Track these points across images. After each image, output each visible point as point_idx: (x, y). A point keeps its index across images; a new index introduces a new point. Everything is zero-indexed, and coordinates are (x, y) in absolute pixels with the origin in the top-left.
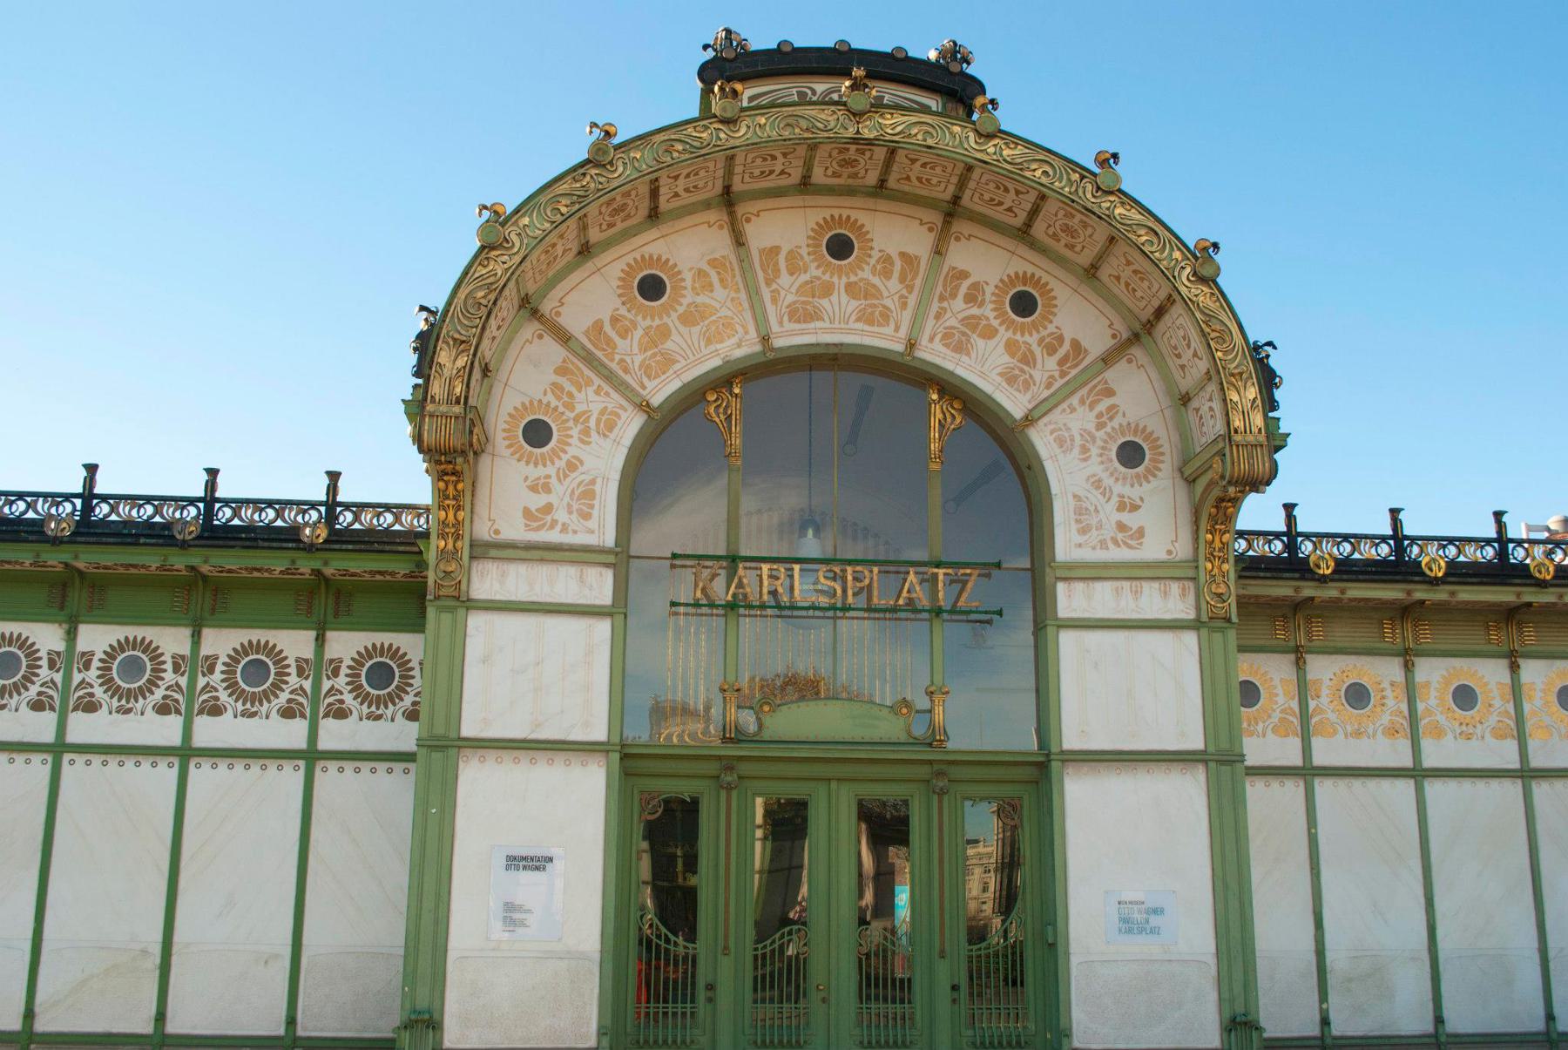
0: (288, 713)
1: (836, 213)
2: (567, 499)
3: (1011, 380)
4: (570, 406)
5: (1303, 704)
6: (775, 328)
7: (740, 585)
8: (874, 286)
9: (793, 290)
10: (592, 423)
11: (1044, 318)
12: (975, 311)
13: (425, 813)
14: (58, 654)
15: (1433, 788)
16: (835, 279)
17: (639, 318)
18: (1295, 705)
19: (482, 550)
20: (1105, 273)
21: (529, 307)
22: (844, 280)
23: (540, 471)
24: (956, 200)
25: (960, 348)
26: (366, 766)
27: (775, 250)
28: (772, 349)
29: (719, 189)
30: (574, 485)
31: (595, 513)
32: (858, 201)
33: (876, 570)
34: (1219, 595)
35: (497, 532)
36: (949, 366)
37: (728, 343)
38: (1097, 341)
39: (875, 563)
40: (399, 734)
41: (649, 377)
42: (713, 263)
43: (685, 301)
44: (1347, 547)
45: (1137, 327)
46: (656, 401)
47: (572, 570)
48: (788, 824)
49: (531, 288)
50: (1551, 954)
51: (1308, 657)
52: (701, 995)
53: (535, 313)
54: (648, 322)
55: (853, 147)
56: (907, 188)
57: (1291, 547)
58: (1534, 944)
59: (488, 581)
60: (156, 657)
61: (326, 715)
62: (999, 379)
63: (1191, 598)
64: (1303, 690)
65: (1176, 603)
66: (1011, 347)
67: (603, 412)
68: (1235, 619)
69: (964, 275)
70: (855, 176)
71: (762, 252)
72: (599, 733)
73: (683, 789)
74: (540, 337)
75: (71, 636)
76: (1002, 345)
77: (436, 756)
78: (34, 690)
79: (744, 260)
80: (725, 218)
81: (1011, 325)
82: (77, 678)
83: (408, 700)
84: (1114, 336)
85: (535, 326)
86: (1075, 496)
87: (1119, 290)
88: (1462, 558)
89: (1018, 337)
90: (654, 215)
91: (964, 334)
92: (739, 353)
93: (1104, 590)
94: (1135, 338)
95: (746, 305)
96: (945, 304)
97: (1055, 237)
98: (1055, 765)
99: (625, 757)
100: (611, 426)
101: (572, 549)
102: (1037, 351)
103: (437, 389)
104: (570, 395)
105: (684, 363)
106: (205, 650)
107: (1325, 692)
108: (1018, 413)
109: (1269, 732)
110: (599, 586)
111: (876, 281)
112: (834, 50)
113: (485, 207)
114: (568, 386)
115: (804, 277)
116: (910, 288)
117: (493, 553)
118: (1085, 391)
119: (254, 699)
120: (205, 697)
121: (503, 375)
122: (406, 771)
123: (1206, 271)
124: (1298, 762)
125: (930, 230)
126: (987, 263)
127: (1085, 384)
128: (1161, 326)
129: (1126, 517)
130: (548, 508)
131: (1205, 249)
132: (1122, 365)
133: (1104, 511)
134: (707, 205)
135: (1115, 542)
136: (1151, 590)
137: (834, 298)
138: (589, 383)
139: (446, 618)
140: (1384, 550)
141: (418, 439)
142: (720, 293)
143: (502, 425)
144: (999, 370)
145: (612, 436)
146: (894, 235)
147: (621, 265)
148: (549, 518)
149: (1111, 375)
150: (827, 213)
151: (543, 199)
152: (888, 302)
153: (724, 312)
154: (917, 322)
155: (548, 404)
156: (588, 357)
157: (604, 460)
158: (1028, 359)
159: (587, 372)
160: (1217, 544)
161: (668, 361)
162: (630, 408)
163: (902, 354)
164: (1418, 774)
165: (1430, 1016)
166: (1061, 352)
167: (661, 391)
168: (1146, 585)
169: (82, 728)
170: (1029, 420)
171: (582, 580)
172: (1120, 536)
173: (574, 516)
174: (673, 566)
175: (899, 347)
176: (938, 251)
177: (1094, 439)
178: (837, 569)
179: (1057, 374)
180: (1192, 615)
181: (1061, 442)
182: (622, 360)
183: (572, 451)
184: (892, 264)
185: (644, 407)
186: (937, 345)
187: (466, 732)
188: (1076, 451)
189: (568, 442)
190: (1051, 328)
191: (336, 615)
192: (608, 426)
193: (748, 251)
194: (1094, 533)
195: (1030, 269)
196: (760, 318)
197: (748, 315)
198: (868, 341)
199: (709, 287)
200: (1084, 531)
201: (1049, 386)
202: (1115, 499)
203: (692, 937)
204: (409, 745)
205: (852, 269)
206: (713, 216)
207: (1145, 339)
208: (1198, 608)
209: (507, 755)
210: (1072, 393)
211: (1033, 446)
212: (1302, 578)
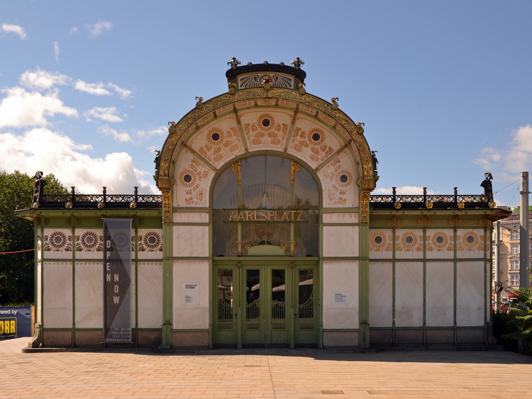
3: (312, 158)
4: (196, 171)
5: (394, 243)
6: (249, 146)
7: (241, 216)
11: (322, 141)
12: (303, 140)
13: (166, 275)
15: (428, 264)
16: (265, 132)
18: (391, 243)
19: (176, 210)
21: (184, 145)
23: (189, 189)
25: (299, 150)
31: (203, 199)
36: (296, 155)
38: (336, 147)
40: (158, 255)
42: (232, 129)
43: (225, 140)
47: (198, 214)
48: (253, 277)
50: (457, 307)
52: (234, 317)
53: (185, 145)
54: (215, 147)
59: (177, 218)
63: (357, 217)
64: (394, 238)
65: (354, 219)
66: (313, 149)
67: (204, 172)
69: (300, 129)
71: (245, 125)
72: (207, 255)
75: (73, 232)
77: (168, 261)
78: (66, 246)
79: (241, 128)
83: (160, 246)
89: (314, 146)
90: (215, 116)
92: (239, 154)
93: (335, 215)
95: (241, 140)
98: (321, 261)
99: (214, 261)
100: (206, 175)
101: (198, 208)
102: (319, 150)
104: (196, 168)
107: (400, 239)
108: (314, 168)
110: (206, 218)
111: (276, 132)
112: (263, 64)
114: (195, 166)
115: (257, 132)
116: (285, 134)
117: (178, 210)
118: (332, 161)
121: (178, 164)
122: (160, 264)
126: (306, 125)
129: (342, 196)
130: (191, 198)
132: (342, 154)
133: (337, 195)
134: (230, 113)
135: (339, 203)
136: (347, 216)
137: (265, 137)
138: (200, 164)
139: (168, 227)
142: (234, 137)
143: (178, 177)
147: (207, 131)
150: (262, 113)
152: (279, 138)
153: (235, 143)
156: (200, 157)
157: (206, 184)
158: (317, 152)
159: (200, 161)
160: (365, 203)
161: (221, 157)
164: (425, 260)
165: (422, 322)
167: (219, 165)
168: (346, 214)
169: (79, 255)
170: (317, 169)
172: (340, 201)
173: (198, 200)
175: (283, 151)
176: (293, 122)
177: (334, 174)
180: (357, 222)
181: (325, 175)
183: (197, 183)
186: (293, 149)
187: (175, 255)
188: (329, 178)
189: (196, 180)
190: (324, 144)
192: (206, 175)
193: (241, 125)
194: (333, 200)
195: (318, 127)
196: (245, 144)
197: (242, 143)
198: (274, 149)
199: (231, 136)
200: (330, 200)
201: (322, 160)
202: (339, 191)
204: (161, 257)
205: (269, 129)
207: (349, 146)
209: (184, 261)
210: (329, 162)
212: (392, 210)
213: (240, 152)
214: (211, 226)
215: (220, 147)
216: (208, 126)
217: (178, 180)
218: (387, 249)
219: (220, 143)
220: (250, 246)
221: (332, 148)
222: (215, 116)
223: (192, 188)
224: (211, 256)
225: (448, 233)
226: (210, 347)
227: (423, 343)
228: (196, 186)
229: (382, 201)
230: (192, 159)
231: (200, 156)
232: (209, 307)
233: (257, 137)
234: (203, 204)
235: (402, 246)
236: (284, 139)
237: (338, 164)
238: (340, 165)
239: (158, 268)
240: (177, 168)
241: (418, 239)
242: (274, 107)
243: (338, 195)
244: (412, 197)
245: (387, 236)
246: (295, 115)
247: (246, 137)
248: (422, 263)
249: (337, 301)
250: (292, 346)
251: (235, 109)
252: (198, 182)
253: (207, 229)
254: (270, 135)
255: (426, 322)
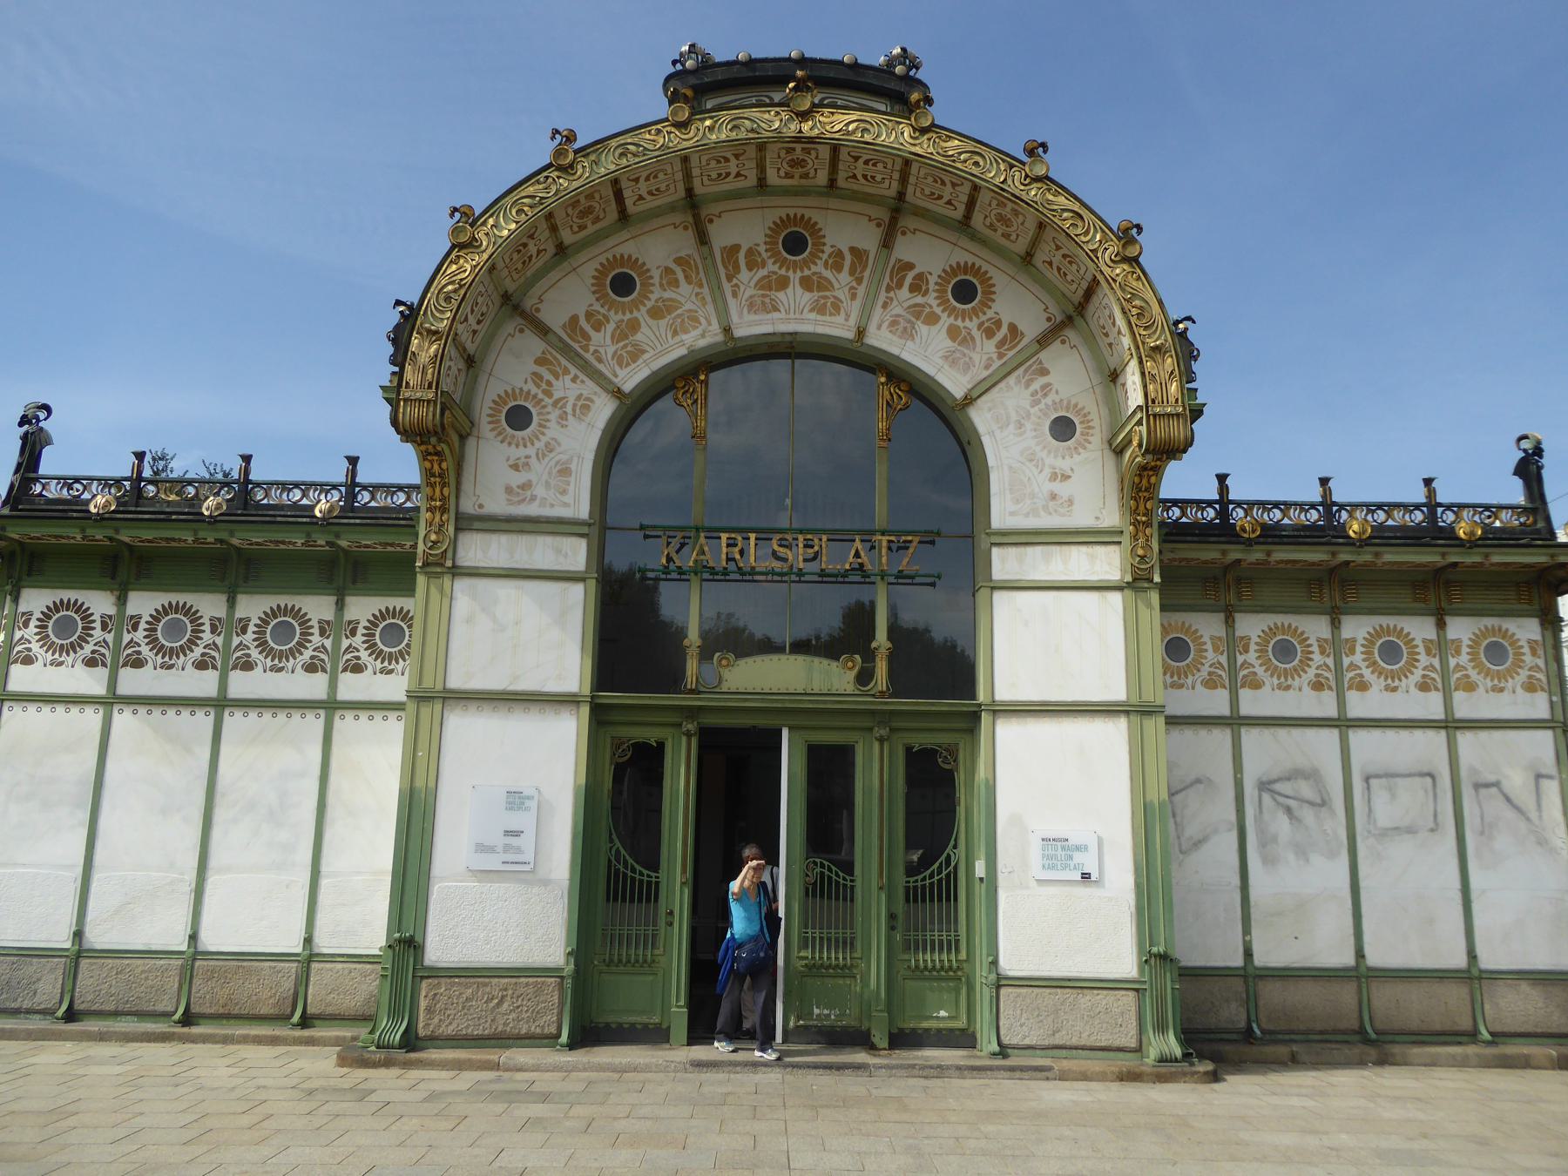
0: (311, 668)
1: (792, 212)
2: (545, 477)
3: (954, 363)
4: (548, 394)
5: (1232, 660)
6: (735, 318)
8: (826, 279)
9: (752, 284)
10: (569, 409)
12: (919, 300)
14: (110, 617)
15: (1357, 738)
17: (612, 313)
18: (1223, 659)
20: (1039, 259)
22: (799, 274)
23: (522, 452)
24: (901, 196)
25: (908, 334)
26: (378, 715)
27: (735, 248)
28: (733, 338)
29: (682, 193)
30: (553, 463)
31: (571, 488)
32: (809, 201)
33: (824, 538)
34: (1142, 557)
35: (481, 506)
36: (895, 351)
37: (695, 333)
38: (1032, 323)
39: (825, 531)
41: (620, 364)
42: (679, 261)
44: (1277, 514)
45: (1071, 310)
46: (628, 387)
47: (549, 539)
49: (510, 286)
50: (1474, 896)
51: (1238, 616)
55: (798, 147)
56: (855, 187)
57: (1223, 514)
58: (1457, 884)
59: (475, 549)
60: (195, 619)
61: (345, 670)
62: (940, 362)
63: (1117, 562)
66: (953, 333)
67: (579, 397)
68: (1157, 579)
69: (910, 266)
70: (805, 176)
73: (651, 735)
74: (521, 331)
76: (944, 330)
80: (691, 219)
81: (952, 312)
82: (127, 638)
84: (1049, 319)
85: (519, 320)
86: (1010, 468)
87: (1052, 275)
88: (1390, 522)
89: (959, 323)
90: (624, 217)
91: (909, 321)
92: (702, 343)
94: (1068, 321)
95: (709, 299)
96: (892, 294)
97: (992, 227)
100: (586, 408)
102: (976, 333)
103: (410, 375)
104: (549, 384)
105: (652, 352)
106: (239, 614)
108: (959, 393)
109: (1198, 685)
110: (575, 554)
111: (828, 274)
113: (455, 210)
114: (548, 376)
115: (763, 272)
116: (859, 281)
117: (477, 525)
119: (281, 655)
120: (239, 654)
122: (399, 719)
123: (1132, 251)
124: (1226, 712)
125: (879, 225)
126: (930, 254)
127: (1020, 365)
128: (1091, 308)
129: (1057, 487)
130: (526, 486)
131: (1126, 231)
135: (1045, 508)
137: (790, 290)
138: (566, 372)
140: (1313, 515)
141: (394, 422)
142: (685, 288)
144: (941, 353)
145: (588, 419)
146: (846, 231)
147: (595, 264)
148: (529, 493)
149: (1043, 355)
150: (783, 213)
151: (509, 200)
153: (688, 306)
154: (866, 313)
155: (529, 392)
156: (566, 348)
159: (564, 362)
161: (636, 354)
162: (604, 394)
163: (851, 341)
166: (999, 336)
167: (631, 378)
170: (969, 400)
171: (558, 551)
174: (646, 537)
175: (850, 335)
176: (887, 243)
177: (1029, 415)
178: (789, 537)
179: (995, 356)
182: (596, 351)
183: (550, 433)
184: (843, 258)
185: (617, 393)
187: (454, 683)
188: (1012, 427)
190: (990, 314)
191: (354, 582)
192: (585, 407)
195: (970, 259)
197: (710, 308)
198: (820, 330)
199: (676, 283)
201: (987, 368)
202: (1047, 471)
203: (655, 867)
205: (806, 263)
206: (678, 218)
207: (1078, 321)
208: (1123, 571)
211: (972, 423)
213: (703, 336)
214: (592, 584)
215: (636, 319)
216: (595, 250)
217: (485, 420)
218: (1211, 683)
219: (636, 305)
220: (731, 656)
221: (1020, 327)
222: (624, 217)
223: (531, 451)
224: (587, 690)
225: (1420, 629)
226: (564, 1038)
227: (1361, 1031)
228: (547, 444)
229: (1184, 520)
230: (539, 354)
231: (567, 345)
232: (571, 879)
233: (762, 288)
234: (566, 505)
235: (1260, 671)
236: (854, 297)
237: (1043, 380)
238: (1049, 384)
239: (393, 730)
240: (482, 379)
241: (1315, 648)
242: (820, 194)
243: (1043, 485)
244: (1284, 506)
245: (1206, 639)
246: (894, 221)
247: (727, 287)
248: (1336, 732)
249: (1052, 867)
250: (880, 1039)
251: (690, 192)
252: (553, 431)
253: (577, 592)
254: (806, 283)
255: (1368, 950)
